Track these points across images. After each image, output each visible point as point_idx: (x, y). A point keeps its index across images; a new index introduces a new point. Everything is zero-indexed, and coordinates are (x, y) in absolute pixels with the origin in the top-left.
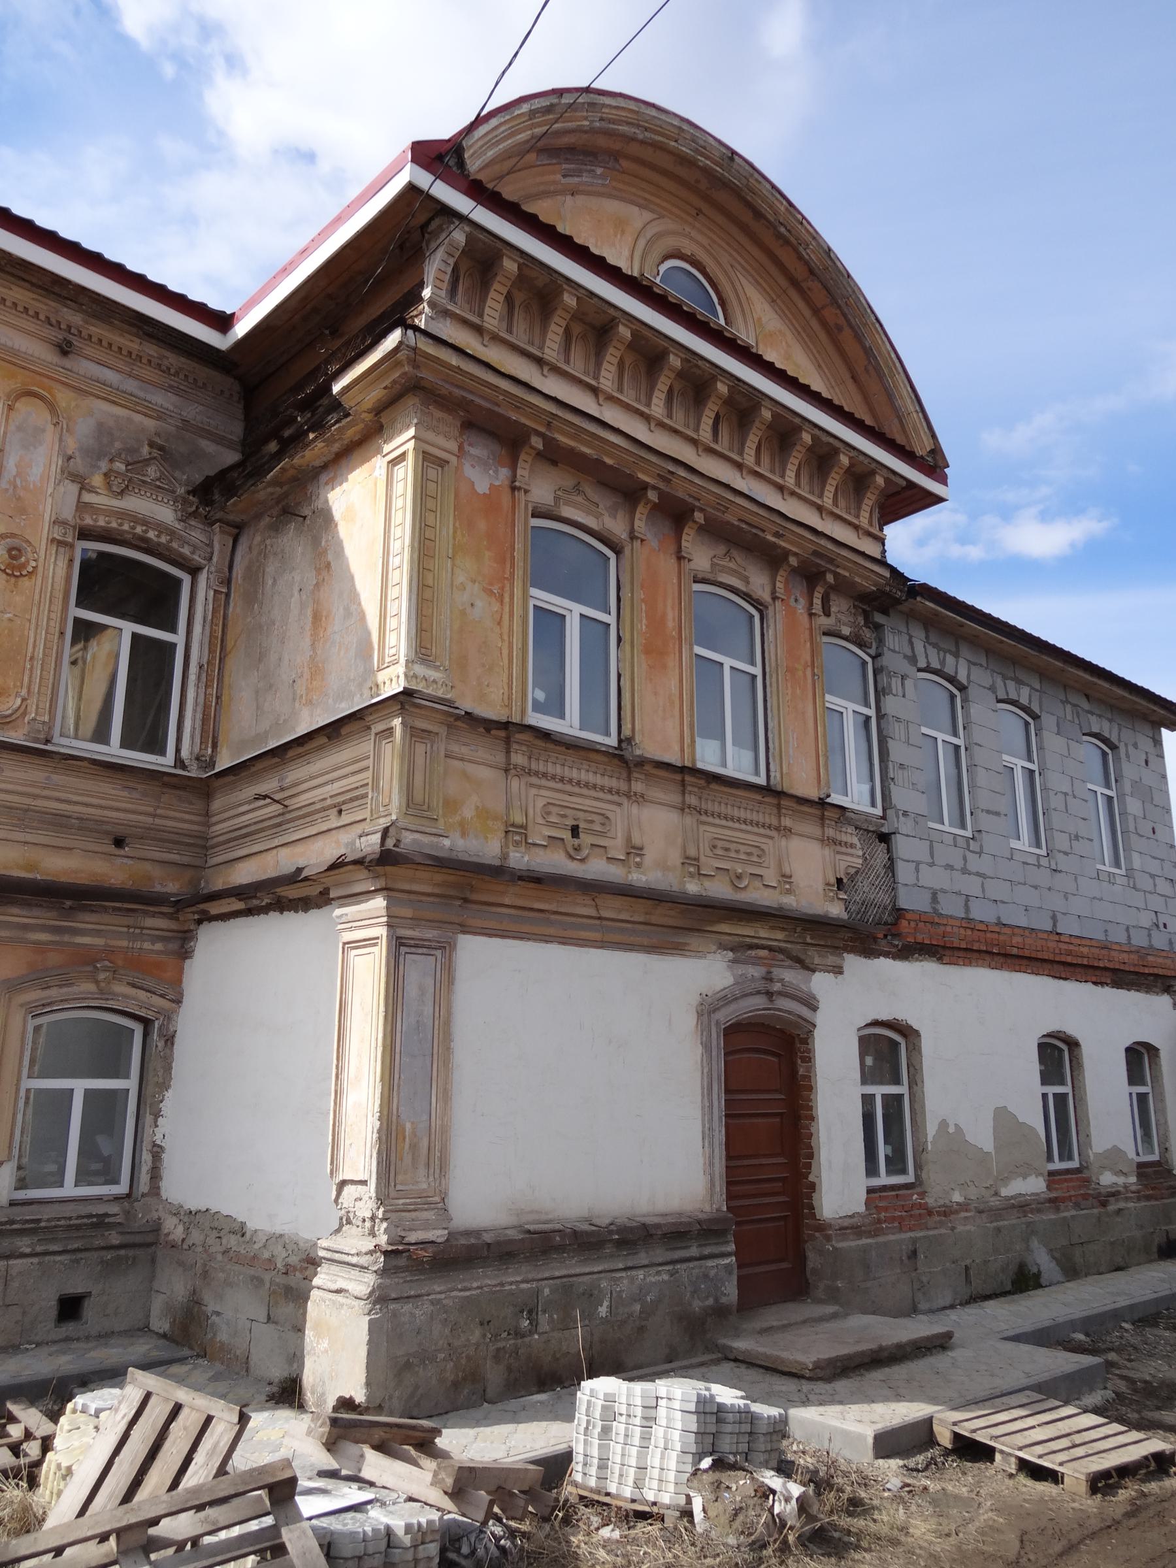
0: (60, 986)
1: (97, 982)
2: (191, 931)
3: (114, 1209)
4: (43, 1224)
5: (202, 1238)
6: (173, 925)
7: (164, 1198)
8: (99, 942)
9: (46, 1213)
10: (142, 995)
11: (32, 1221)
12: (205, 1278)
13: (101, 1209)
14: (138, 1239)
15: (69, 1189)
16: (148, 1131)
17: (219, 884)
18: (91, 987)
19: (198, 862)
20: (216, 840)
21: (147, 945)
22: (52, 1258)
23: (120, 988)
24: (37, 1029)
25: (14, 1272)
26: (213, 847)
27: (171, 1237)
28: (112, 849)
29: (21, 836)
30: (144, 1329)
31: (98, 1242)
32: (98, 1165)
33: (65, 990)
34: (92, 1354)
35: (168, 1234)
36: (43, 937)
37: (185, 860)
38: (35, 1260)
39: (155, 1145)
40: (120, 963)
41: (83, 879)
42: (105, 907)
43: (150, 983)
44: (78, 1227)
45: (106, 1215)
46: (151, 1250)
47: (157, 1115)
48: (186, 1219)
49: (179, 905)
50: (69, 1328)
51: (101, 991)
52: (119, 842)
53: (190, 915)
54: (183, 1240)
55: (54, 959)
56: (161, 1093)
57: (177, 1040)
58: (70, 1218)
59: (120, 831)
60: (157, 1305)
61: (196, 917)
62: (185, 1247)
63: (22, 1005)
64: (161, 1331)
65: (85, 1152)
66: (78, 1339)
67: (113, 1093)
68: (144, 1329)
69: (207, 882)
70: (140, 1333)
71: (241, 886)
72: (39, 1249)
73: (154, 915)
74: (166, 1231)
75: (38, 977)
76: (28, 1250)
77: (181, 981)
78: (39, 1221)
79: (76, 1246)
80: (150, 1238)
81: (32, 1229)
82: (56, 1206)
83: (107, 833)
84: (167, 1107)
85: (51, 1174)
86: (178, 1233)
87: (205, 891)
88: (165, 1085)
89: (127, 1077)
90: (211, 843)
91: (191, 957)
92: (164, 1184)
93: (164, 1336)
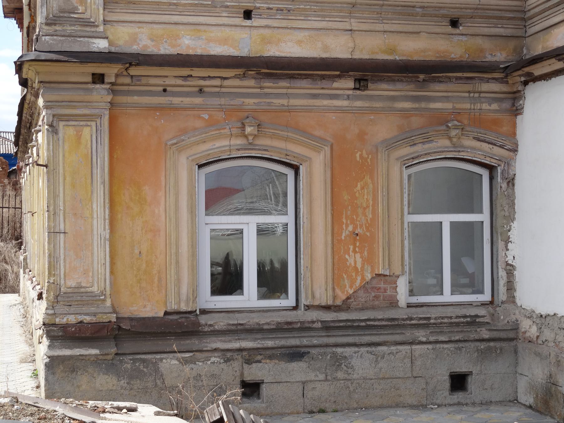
0: (423, 143)
1: (450, 138)
2: (519, 91)
3: (482, 312)
4: (432, 321)
5: (553, 336)
6: (503, 88)
7: (519, 304)
8: (449, 106)
9: (434, 313)
10: (485, 146)
11: (425, 319)
12: (558, 366)
13: (473, 312)
14: (503, 335)
15: (447, 297)
16: (501, 253)
17: (539, 50)
18: (447, 142)
19: (520, 33)
20: (537, 10)
21: (485, 106)
22: (442, 346)
23: (468, 142)
24: (409, 176)
25: (417, 354)
26: (531, 18)
27: (528, 335)
28: (450, 29)
29: (380, 27)
30: (515, 401)
31: (473, 336)
32: (467, 281)
33: (427, 146)
34: (478, 415)
35: (525, 332)
36: (407, 105)
37: (509, 32)
38: (430, 346)
39: (508, 264)
40: (466, 122)
41: (430, 56)
42: (449, 78)
43: (490, 137)
44: (457, 324)
45: (477, 316)
46: (513, 343)
47: (507, 241)
48: (538, 321)
49: (508, 70)
50: (459, 396)
51: (454, 146)
52: (454, 23)
53: (517, 78)
54: (538, 337)
55: (416, 121)
56: (508, 224)
57: (517, 181)
58: (451, 318)
59: (455, 13)
60: (522, 384)
61: (523, 79)
62: (540, 342)
63: (397, 159)
64: (527, 404)
65: (457, 269)
66: (467, 404)
67: (470, 225)
68: (515, 401)
69: (528, 49)
70: (512, 404)
71: (558, 49)
72: (432, 339)
73: (488, 80)
74: (523, 330)
75: (406, 137)
76: (424, 339)
77: (515, 134)
78: (429, 318)
79: (457, 338)
80: (511, 335)
81: (425, 324)
82: (440, 309)
83: (444, 16)
84: (513, 235)
85: (434, 286)
86: (533, 331)
87: (528, 57)
88: (511, 218)
89: (481, 212)
90: (529, 14)
91: (521, 114)
92: (517, 294)
93: (530, 407)
